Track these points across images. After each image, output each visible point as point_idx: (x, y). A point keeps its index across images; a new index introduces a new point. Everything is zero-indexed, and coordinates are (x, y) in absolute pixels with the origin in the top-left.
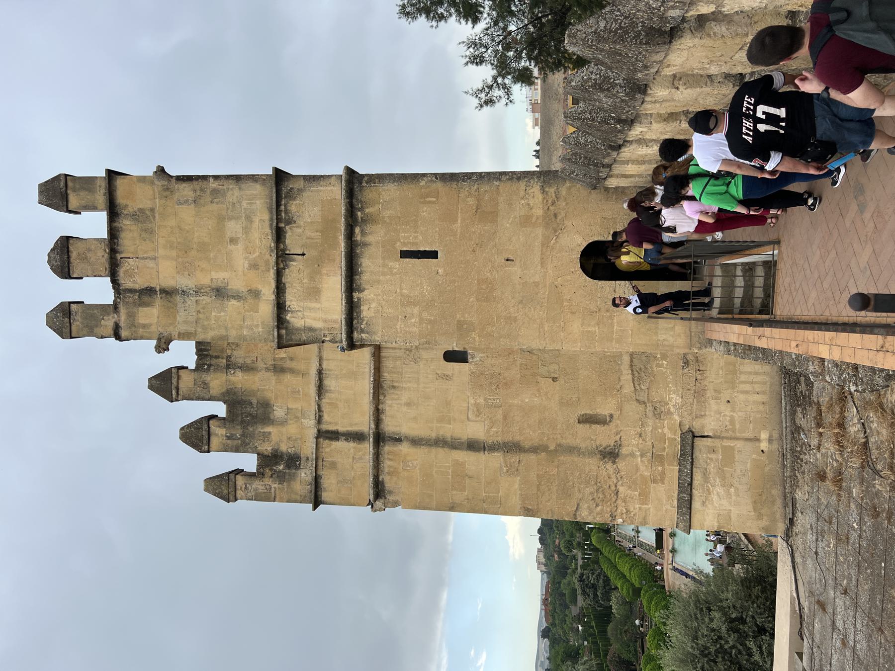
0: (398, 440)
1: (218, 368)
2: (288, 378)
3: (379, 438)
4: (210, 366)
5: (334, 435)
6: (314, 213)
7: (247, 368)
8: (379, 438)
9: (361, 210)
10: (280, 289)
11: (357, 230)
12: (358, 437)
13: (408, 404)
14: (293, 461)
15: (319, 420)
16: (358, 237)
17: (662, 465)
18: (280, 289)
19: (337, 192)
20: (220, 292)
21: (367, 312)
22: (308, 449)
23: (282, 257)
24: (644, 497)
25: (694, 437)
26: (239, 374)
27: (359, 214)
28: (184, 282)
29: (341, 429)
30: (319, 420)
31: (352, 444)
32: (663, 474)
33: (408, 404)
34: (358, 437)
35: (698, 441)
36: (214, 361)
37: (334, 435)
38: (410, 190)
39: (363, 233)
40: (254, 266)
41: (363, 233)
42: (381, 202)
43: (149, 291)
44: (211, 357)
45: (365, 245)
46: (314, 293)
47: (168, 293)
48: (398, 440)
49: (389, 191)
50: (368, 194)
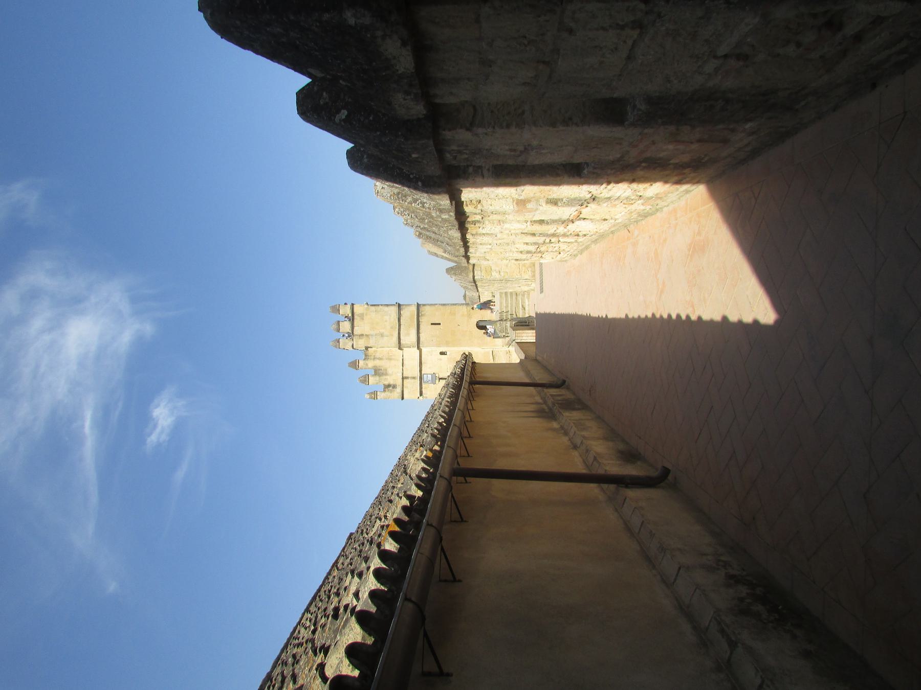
2: (392, 361)
5: (407, 378)
6: (409, 313)
7: (380, 359)
10: (399, 334)
12: (414, 378)
14: (394, 387)
18: (399, 334)
19: (414, 309)
20: (382, 335)
21: (421, 339)
22: (399, 382)
23: (400, 325)
28: (372, 332)
31: (413, 381)
34: (414, 378)
37: (407, 378)
38: (433, 308)
40: (392, 328)
42: (426, 310)
43: (362, 335)
46: (408, 334)
47: (367, 336)
49: (427, 308)
50: (422, 309)
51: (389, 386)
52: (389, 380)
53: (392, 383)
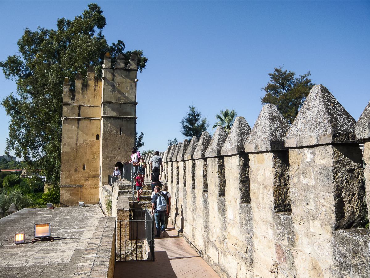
0: (78, 123)
1: (95, 83)
3: (79, 120)
4: (95, 81)
8: (79, 120)
9: (129, 120)
11: (125, 119)
12: (79, 115)
13: (86, 126)
14: (73, 99)
15: (83, 106)
16: (124, 119)
17: (74, 181)
24: (67, 178)
25: (81, 187)
26: (94, 88)
27: (128, 120)
29: (81, 111)
30: (82, 106)
32: (72, 181)
33: (86, 126)
35: (80, 188)
36: (96, 82)
39: (125, 120)
41: (125, 120)
44: (98, 82)
45: (123, 121)
48: (78, 123)
51: (74, 96)
52: (78, 97)
53: (76, 98)
